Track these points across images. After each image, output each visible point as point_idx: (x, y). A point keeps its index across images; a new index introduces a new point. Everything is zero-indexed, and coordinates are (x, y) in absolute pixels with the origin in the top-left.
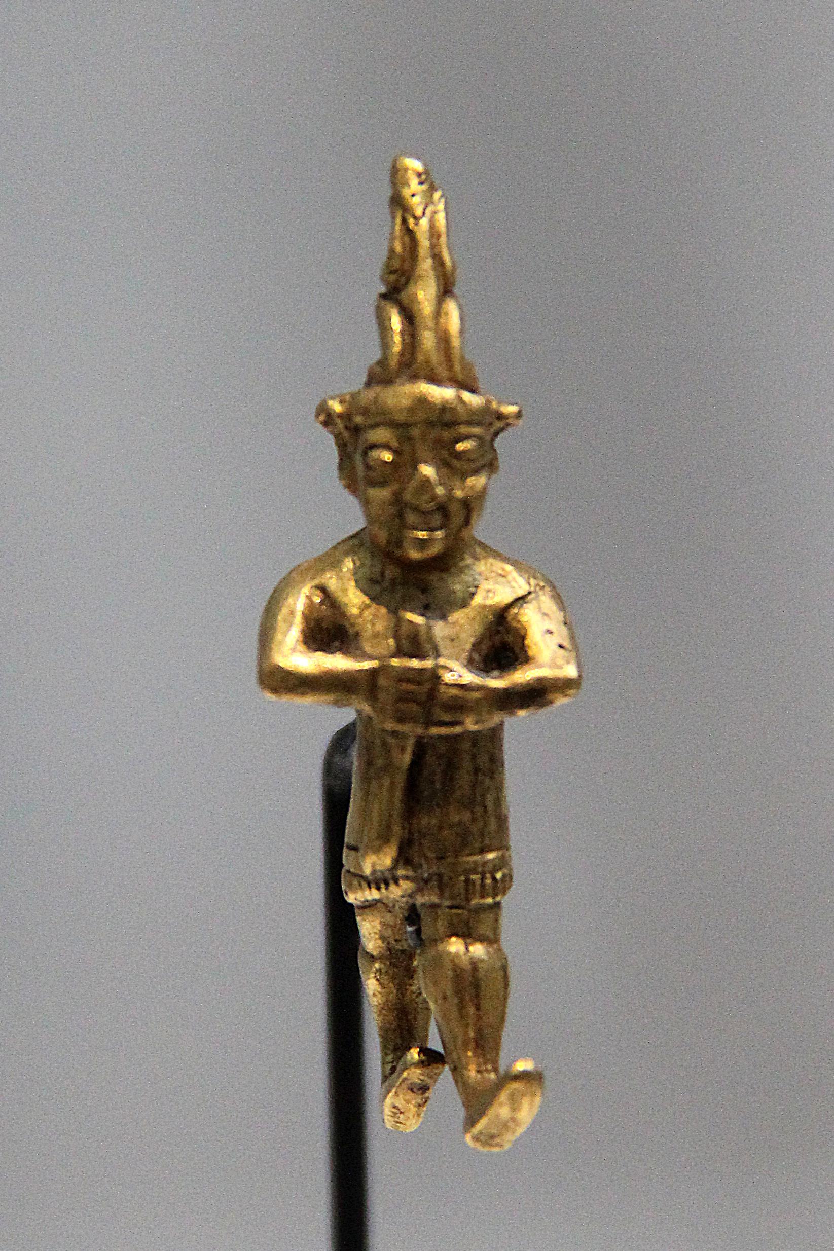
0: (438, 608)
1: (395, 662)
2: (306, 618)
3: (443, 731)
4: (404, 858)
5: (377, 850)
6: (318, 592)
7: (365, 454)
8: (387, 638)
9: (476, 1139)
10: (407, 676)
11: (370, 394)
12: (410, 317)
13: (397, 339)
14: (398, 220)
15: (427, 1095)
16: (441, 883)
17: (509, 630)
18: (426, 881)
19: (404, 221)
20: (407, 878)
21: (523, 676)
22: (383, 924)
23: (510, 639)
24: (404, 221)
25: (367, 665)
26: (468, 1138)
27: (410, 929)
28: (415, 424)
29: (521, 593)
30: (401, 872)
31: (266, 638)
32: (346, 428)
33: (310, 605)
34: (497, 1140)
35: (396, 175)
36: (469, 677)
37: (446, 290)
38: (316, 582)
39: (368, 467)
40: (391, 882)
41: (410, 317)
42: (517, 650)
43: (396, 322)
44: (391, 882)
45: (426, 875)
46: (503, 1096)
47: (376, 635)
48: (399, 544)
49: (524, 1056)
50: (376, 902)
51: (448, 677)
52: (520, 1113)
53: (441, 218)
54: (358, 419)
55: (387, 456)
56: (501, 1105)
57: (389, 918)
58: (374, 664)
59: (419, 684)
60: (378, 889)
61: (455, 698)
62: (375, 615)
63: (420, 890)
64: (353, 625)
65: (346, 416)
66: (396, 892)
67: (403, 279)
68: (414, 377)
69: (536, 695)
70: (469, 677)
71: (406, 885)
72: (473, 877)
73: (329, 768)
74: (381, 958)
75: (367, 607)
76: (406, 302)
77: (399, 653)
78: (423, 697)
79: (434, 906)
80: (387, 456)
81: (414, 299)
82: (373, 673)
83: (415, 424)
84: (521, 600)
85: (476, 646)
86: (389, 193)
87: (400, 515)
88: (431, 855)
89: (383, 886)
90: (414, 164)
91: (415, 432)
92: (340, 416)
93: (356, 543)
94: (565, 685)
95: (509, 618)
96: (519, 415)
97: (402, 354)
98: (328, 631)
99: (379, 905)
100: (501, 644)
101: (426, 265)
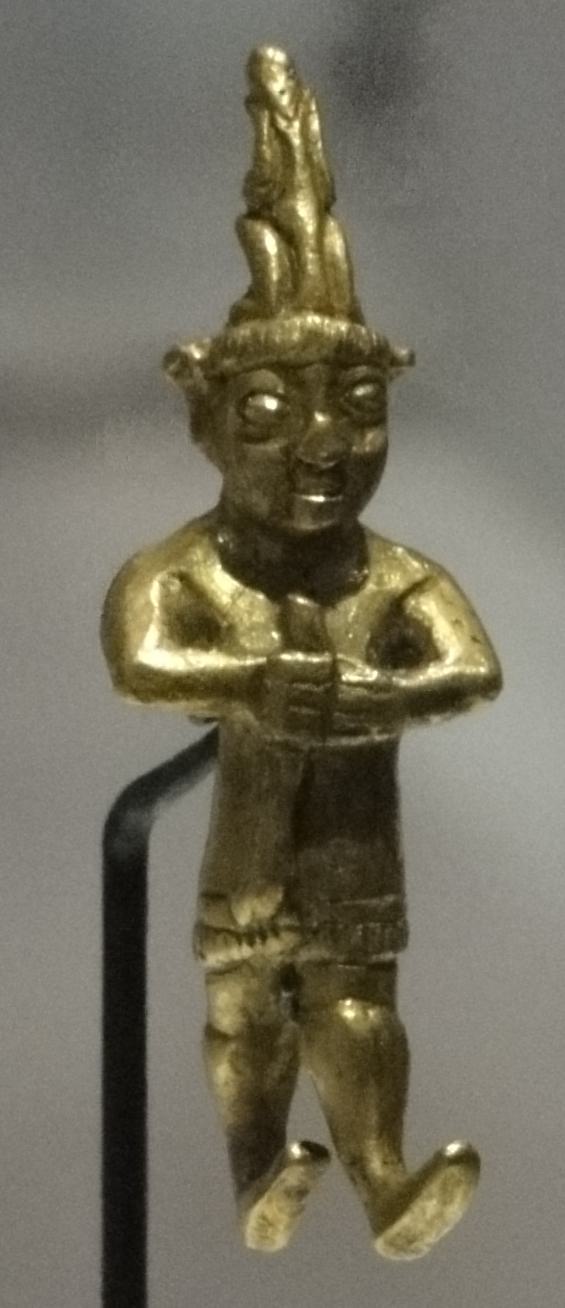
0: (329, 594)
1: (286, 657)
2: (166, 608)
3: (345, 741)
4: (290, 905)
5: (260, 893)
6: (177, 582)
7: (243, 403)
8: (268, 631)
9: (391, 1243)
10: (299, 674)
11: (244, 331)
12: (289, 237)
13: (274, 264)
14: (265, 125)
15: (303, 1202)
16: (332, 933)
17: (410, 621)
18: (315, 932)
19: (273, 123)
20: (290, 929)
22: (247, 993)
23: (411, 632)
24: (273, 123)
25: (250, 662)
26: (379, 1245)
27: (285, 995)
28: (309, 364)
29: (419, 576)
30: (284, 921)
31: (114, 637)
32: (205, 377)
33: (166, 594)
34: (413, 1247)
35: (255, 68)
36: (372, 675)
37: (324, 210)
38: (173, 568)
39: (246, 420)
40: (269, 934)
41: (289, 237)
42: (422, 646)
43: (270, 242)
44: (269, 934)
45: (315, 924)
46: (434, 1187)
47: (253, 628)
48: (288, 511)
49: (451, 1141)
50: (245, 962)
51: (349, 676)
52: (434, 1216)
53: (315, 125)
54: (228, 363)
55: (271, 404)
56: (430, 1197)
57: (254, 983)
58: (262, 660)
59: (317, 683)
60: (251, 944)
61: (361, 700)
62: (252, 604)
63: (304, 944)
64: (224, 616)
66: (274, 947)
67: (275, 194)
68: (299, 309)
69: (452, 697)
70: (372, 675)
71: (289, 939)
72: (372, 925)
73: (114, 826)
74: (238, 1037)
75: (241, 594)
76: (283, 219)
77: (289, 644)
78: (318, 703)
79: (324, 964)
80: (271, 404)
81: (293, 213)
82: (259, 672)
83: (309, 364)
84: (416, 588)
85: (373, 643)
86: (244, 90)
87: (290, 476)
88: (322, 897)
89: (258, 940)
90: (276, 56)
91: (309, 374)
92: (201, 363)
93: (209, 525)
95: (408, 611)
96: (412, 360)
97: (280, 282)
98: (197, 624)
99: (245, 970)
100: (401, 640)
101: (301, 175)
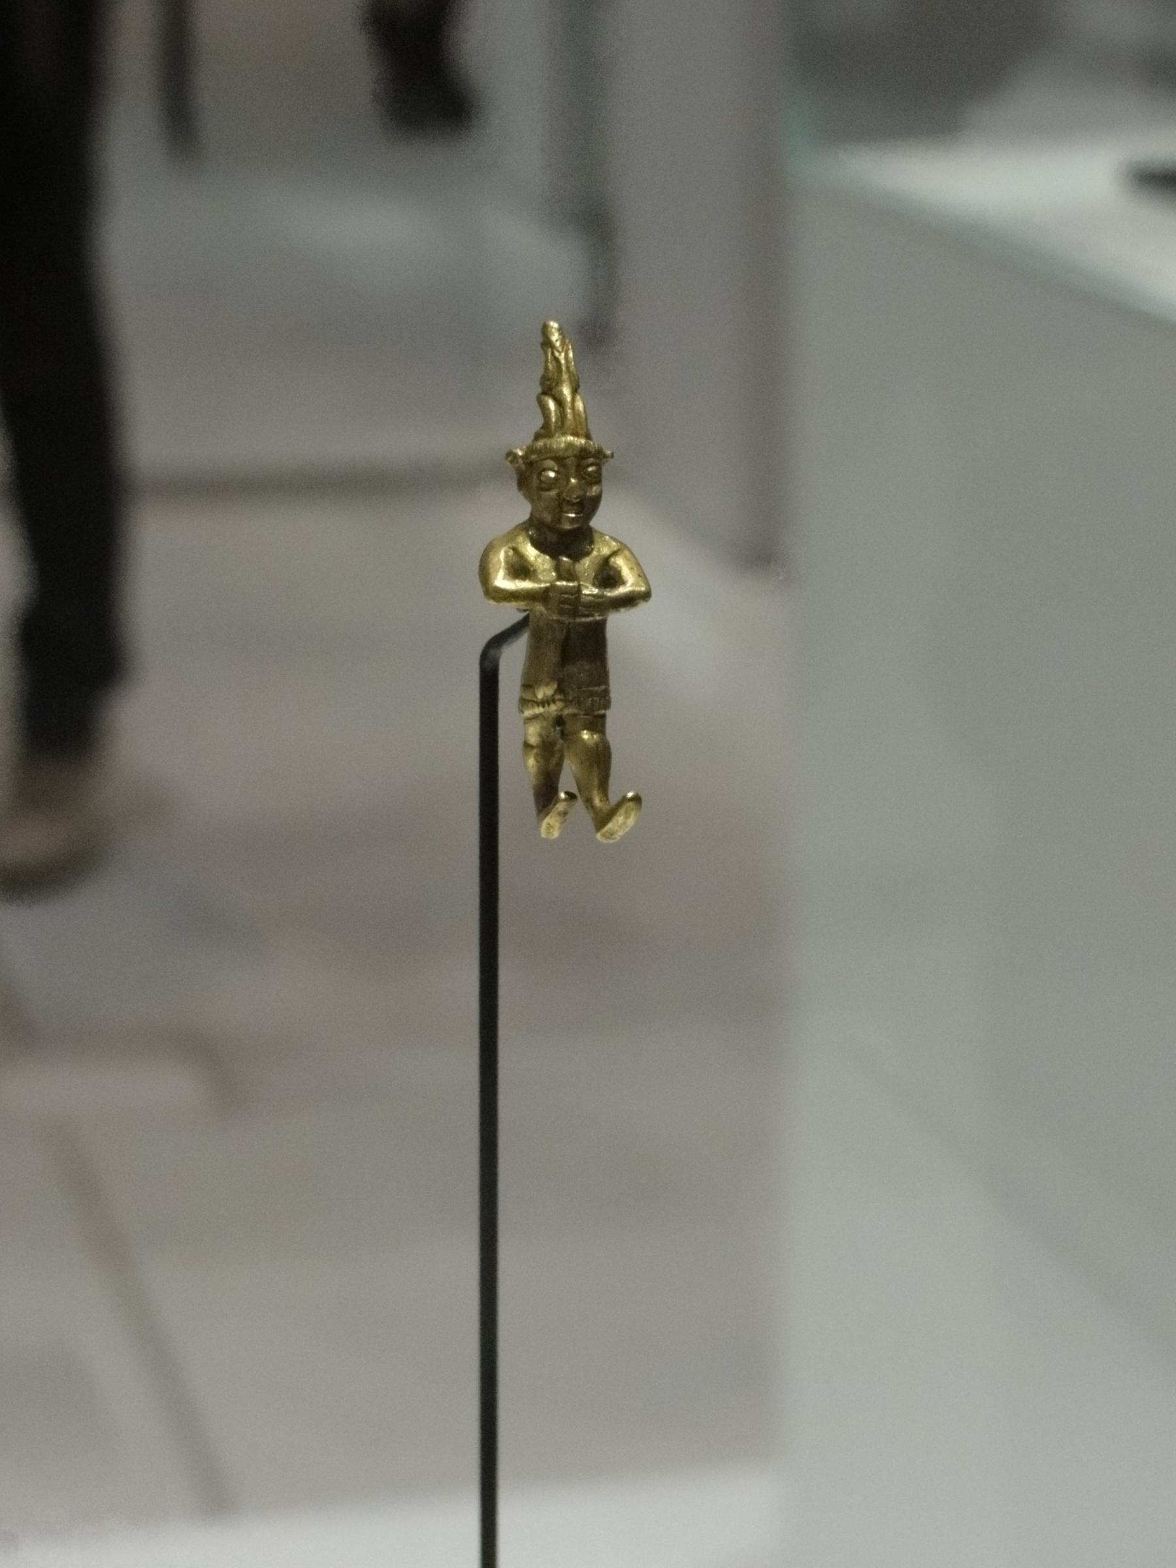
0: (577, 557)
1: (558, 583)
2: (507, 562)
3: (584, 620)
4: (560, 690)
5: (547, 684)
7: (540, 474)
9: (604, 835)
10: (564, 591)
11: (540, 443)
12: (560, 403)
16: (578, 702)
20: (560, 700)
21: (622, 590)
22: (542, 728)
25: (543, 585)
26: (598, 836)
30: (558, 697)
31: (485, 575)
33: (507, 556)
35: (545, 330)
36: (596, 591)
41: (560, 403)
43: (552, 405)
46: (622, 811)
47: (544, 571)
48: (559, 521)
50: (541, 714)
51: (586, 592)
52: (622, 824)
53: (571, 355)
54: (534, 457)
55: (552, 474)
57: (545, 724)
61: (591, 602)
65: (524, 457)
66: (553, 708)
68: (564, 434)
69: (630, 601)
70: (596, 591)
71: (560, 704)
73: (484, 656)
74: (538, 746)
76: (557, 395)
77: (560, 578)
78: (572, 602)
79: (575, 715)
80: (552, 474)
81: (561, 392)
82: (547, 590)
84: (615, 554)
85: (596, 577)
86: (540, 339)
87: (560, 506)
90: (554, 325)
91: (568, 461)
92: (522, 457)
93: (525, 527)
94: (646, 596)
96: (612, 456)
98: (520, 569)
100: (608, 576)
101: (565, 376)
